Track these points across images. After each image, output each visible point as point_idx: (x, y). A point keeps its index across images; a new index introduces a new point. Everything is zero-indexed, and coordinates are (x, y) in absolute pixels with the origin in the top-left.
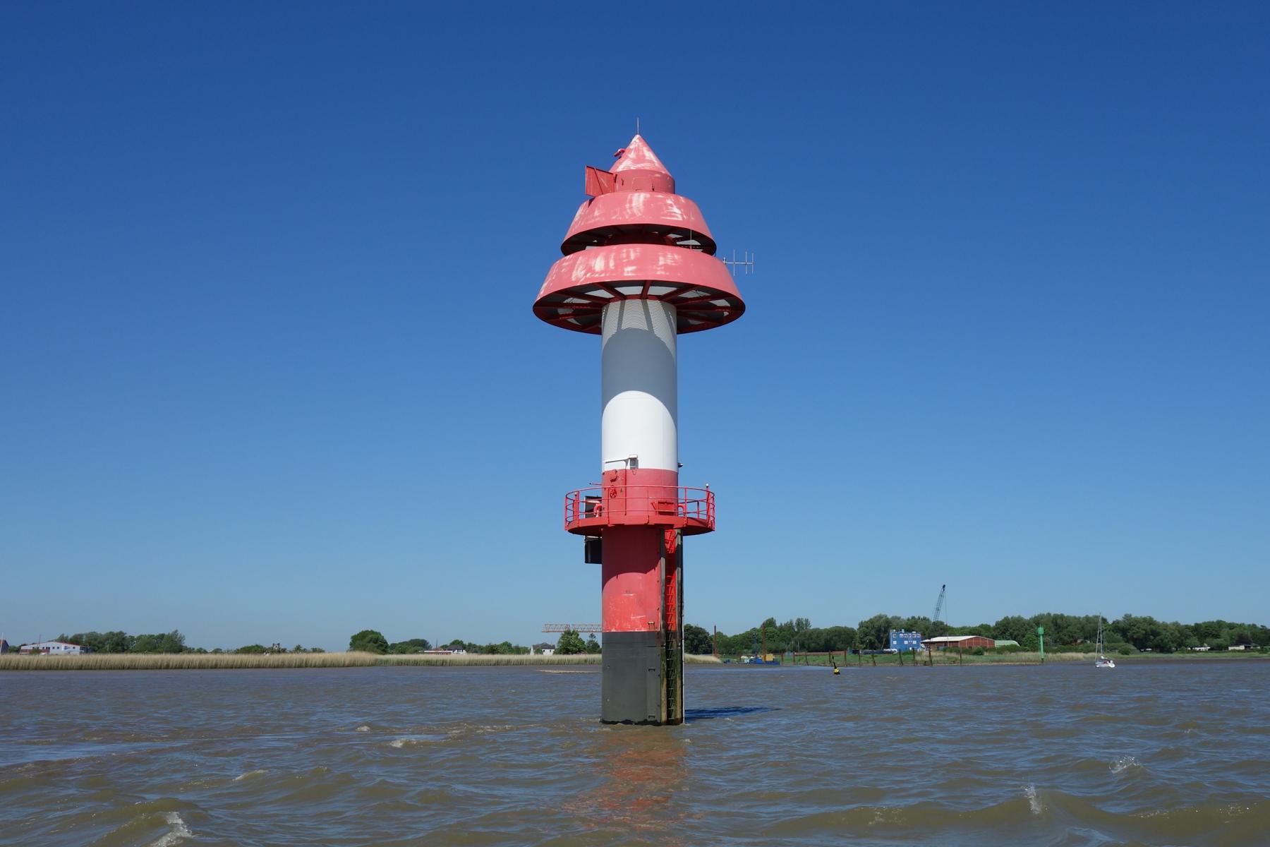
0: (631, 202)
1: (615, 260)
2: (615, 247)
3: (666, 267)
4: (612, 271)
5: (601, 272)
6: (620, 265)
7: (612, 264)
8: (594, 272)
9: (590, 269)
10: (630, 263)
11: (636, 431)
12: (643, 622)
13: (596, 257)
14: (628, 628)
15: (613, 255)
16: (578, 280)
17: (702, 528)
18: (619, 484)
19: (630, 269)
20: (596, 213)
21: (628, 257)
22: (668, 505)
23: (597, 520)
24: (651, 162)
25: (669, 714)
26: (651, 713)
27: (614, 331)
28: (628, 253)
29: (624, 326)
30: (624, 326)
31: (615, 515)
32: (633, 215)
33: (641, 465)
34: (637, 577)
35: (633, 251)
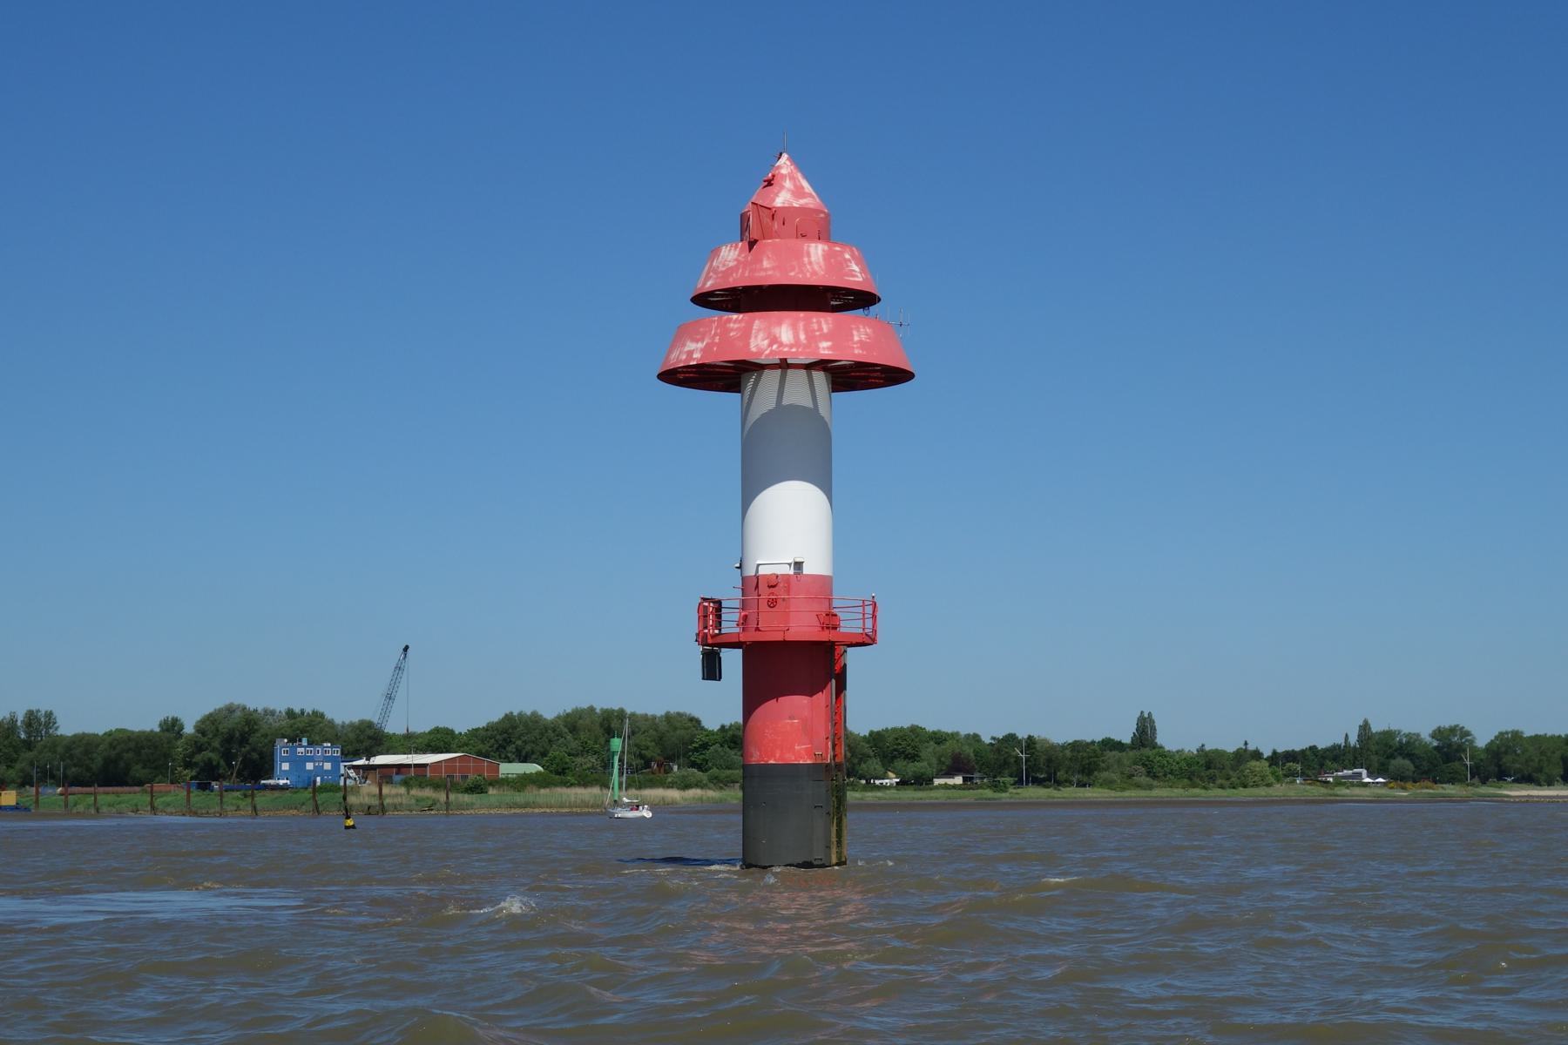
0: (809, 255)
1: (806, 333)
2: (802, 314)
3: (862, 344)
4: (806, 346)
5: (791, 346)
6: (812, 338)
7: (802, 337)
8: (781, 344)
9: (774, 340)
10: (825, 338)
11: (792, 529)
12: (809, 752)
13: (780, 324)
14: (791, 759)
15: (801, 325)
16: (760, 353)
17: (866, 641)
18: (780, 593)
19: (825, 344)
20: (766, 264)
21: (820, 329)
22: (830, 620)
23: (751, 636)
24: (810, 195)
25: (839, 854)
26: (818, 855)
27: (772, 405)
28: (819, 323)
29: (785, 402)
30: (785, 402)
31: (772, 629)
32: (814, 273)
33: (807, 570)
34: (801, 701)
35: (824, 322)
